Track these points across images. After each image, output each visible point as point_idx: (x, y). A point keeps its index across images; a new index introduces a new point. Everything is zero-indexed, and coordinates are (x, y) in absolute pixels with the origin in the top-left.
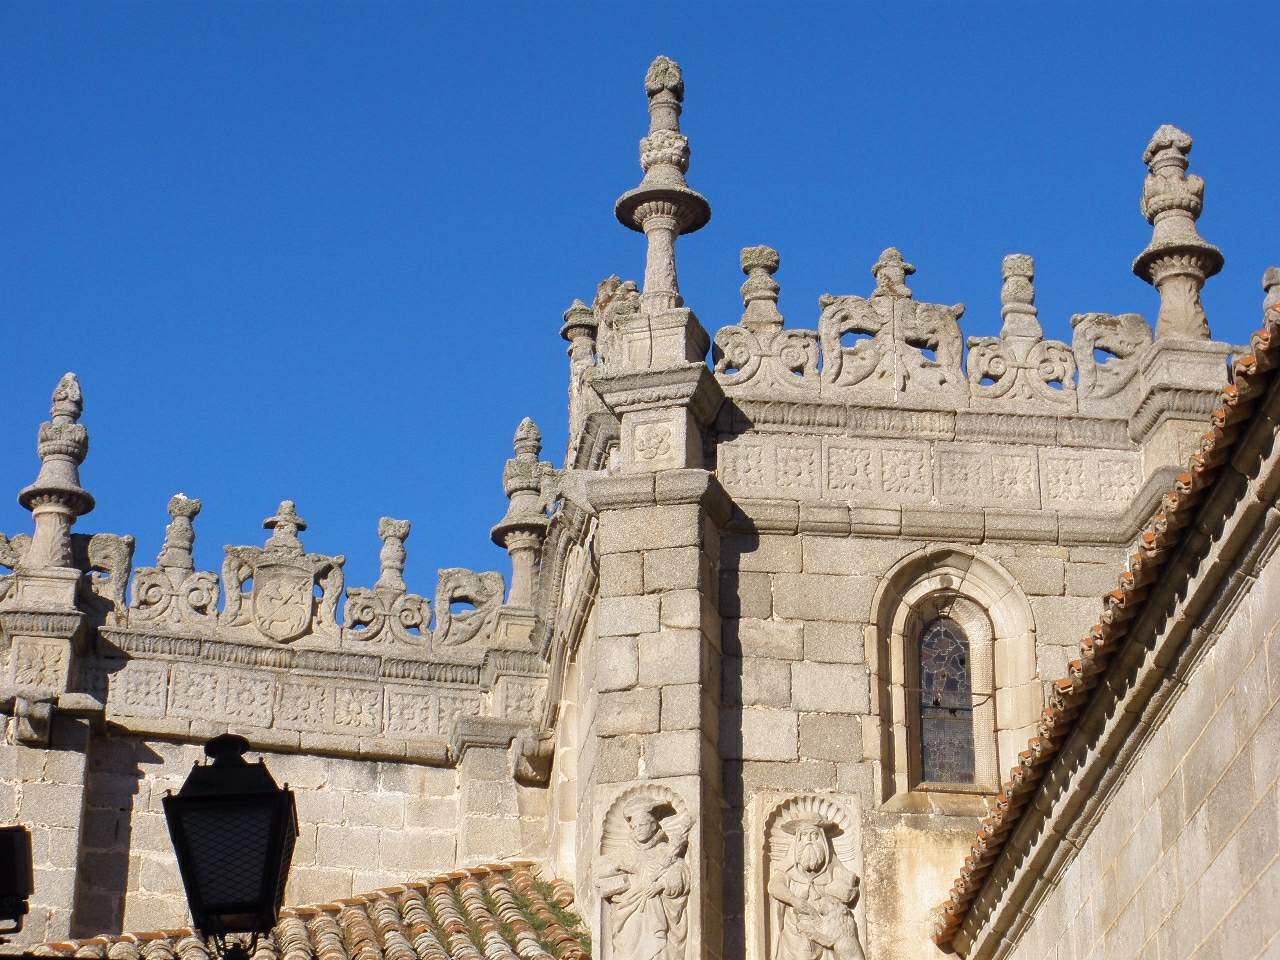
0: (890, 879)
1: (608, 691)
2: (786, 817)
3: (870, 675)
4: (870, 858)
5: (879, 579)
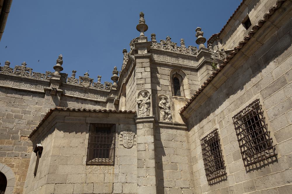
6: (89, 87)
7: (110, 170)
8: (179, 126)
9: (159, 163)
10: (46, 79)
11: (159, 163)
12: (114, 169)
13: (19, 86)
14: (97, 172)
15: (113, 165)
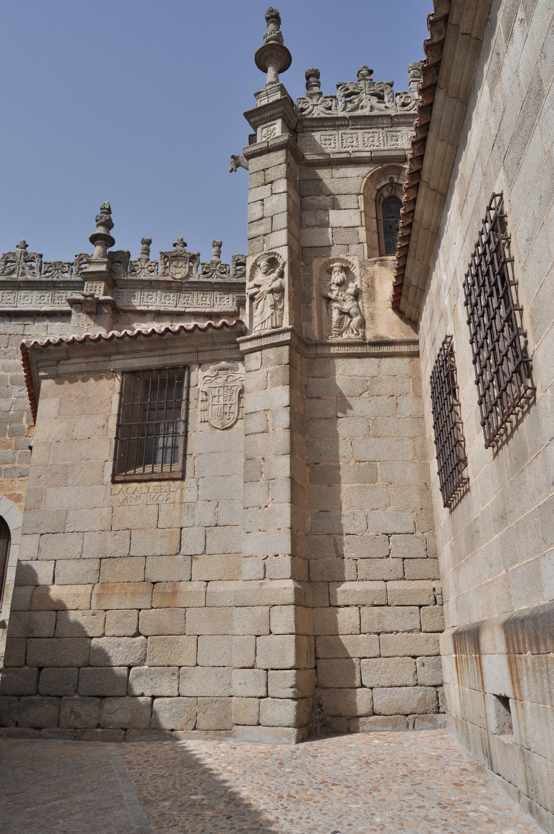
0: (372, 286)
1: (252, 222)
3: (361, 212)
4: (363, 279)
5: (364, 178)
6: (188, 276)
7: (172, 494)
8: (385, 349)
9: (315, 464)
10: (77, 273)
11: (315, 464)
12: (182, 489)
13: (15, 305)
14: (139, 501)
15: (183, 479)
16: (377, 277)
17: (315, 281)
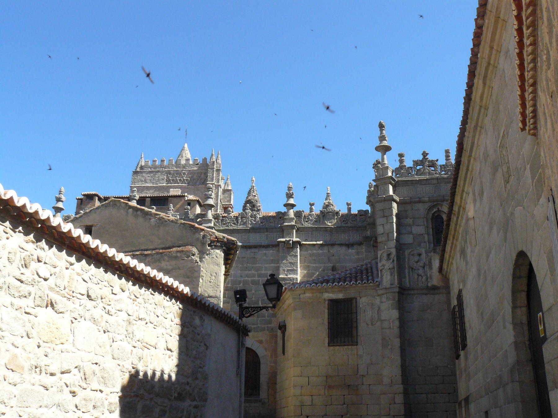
2: (412, 253)
16: (432, 258)
17: (406, 260)
